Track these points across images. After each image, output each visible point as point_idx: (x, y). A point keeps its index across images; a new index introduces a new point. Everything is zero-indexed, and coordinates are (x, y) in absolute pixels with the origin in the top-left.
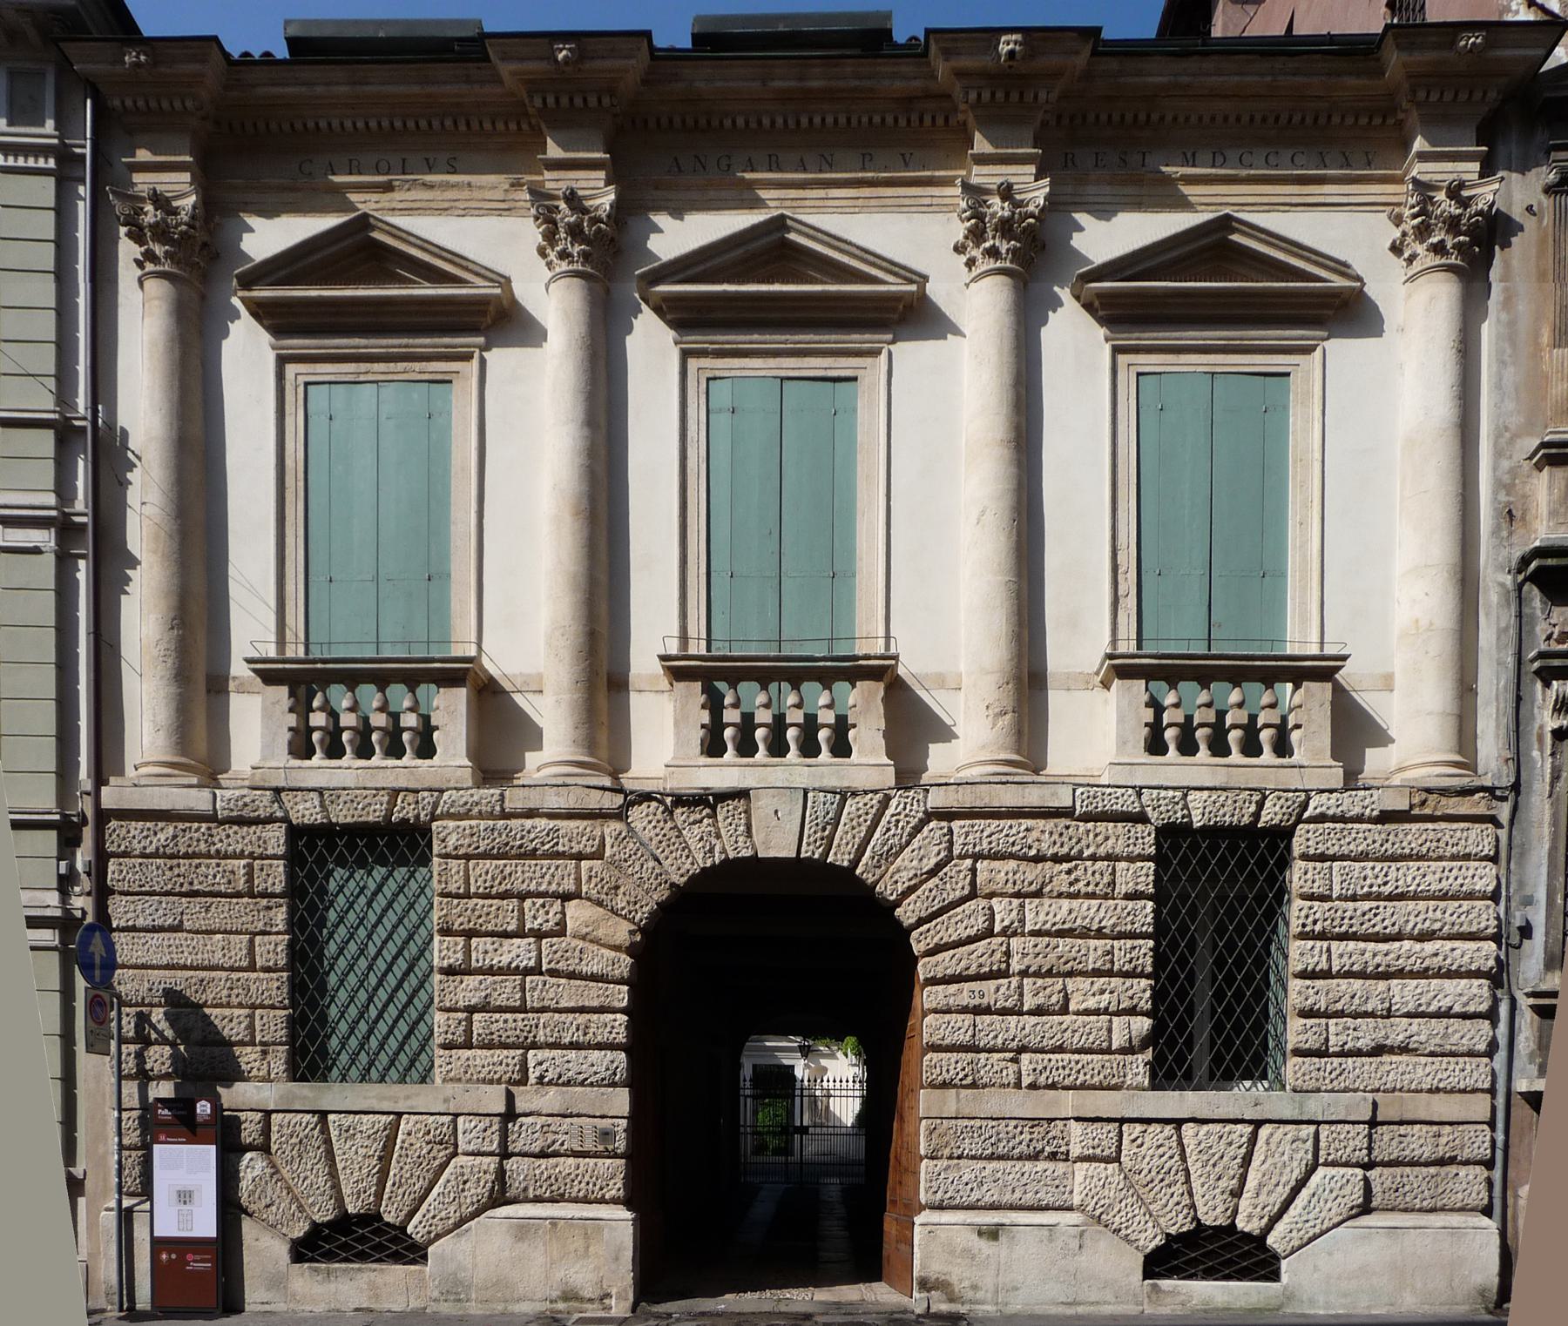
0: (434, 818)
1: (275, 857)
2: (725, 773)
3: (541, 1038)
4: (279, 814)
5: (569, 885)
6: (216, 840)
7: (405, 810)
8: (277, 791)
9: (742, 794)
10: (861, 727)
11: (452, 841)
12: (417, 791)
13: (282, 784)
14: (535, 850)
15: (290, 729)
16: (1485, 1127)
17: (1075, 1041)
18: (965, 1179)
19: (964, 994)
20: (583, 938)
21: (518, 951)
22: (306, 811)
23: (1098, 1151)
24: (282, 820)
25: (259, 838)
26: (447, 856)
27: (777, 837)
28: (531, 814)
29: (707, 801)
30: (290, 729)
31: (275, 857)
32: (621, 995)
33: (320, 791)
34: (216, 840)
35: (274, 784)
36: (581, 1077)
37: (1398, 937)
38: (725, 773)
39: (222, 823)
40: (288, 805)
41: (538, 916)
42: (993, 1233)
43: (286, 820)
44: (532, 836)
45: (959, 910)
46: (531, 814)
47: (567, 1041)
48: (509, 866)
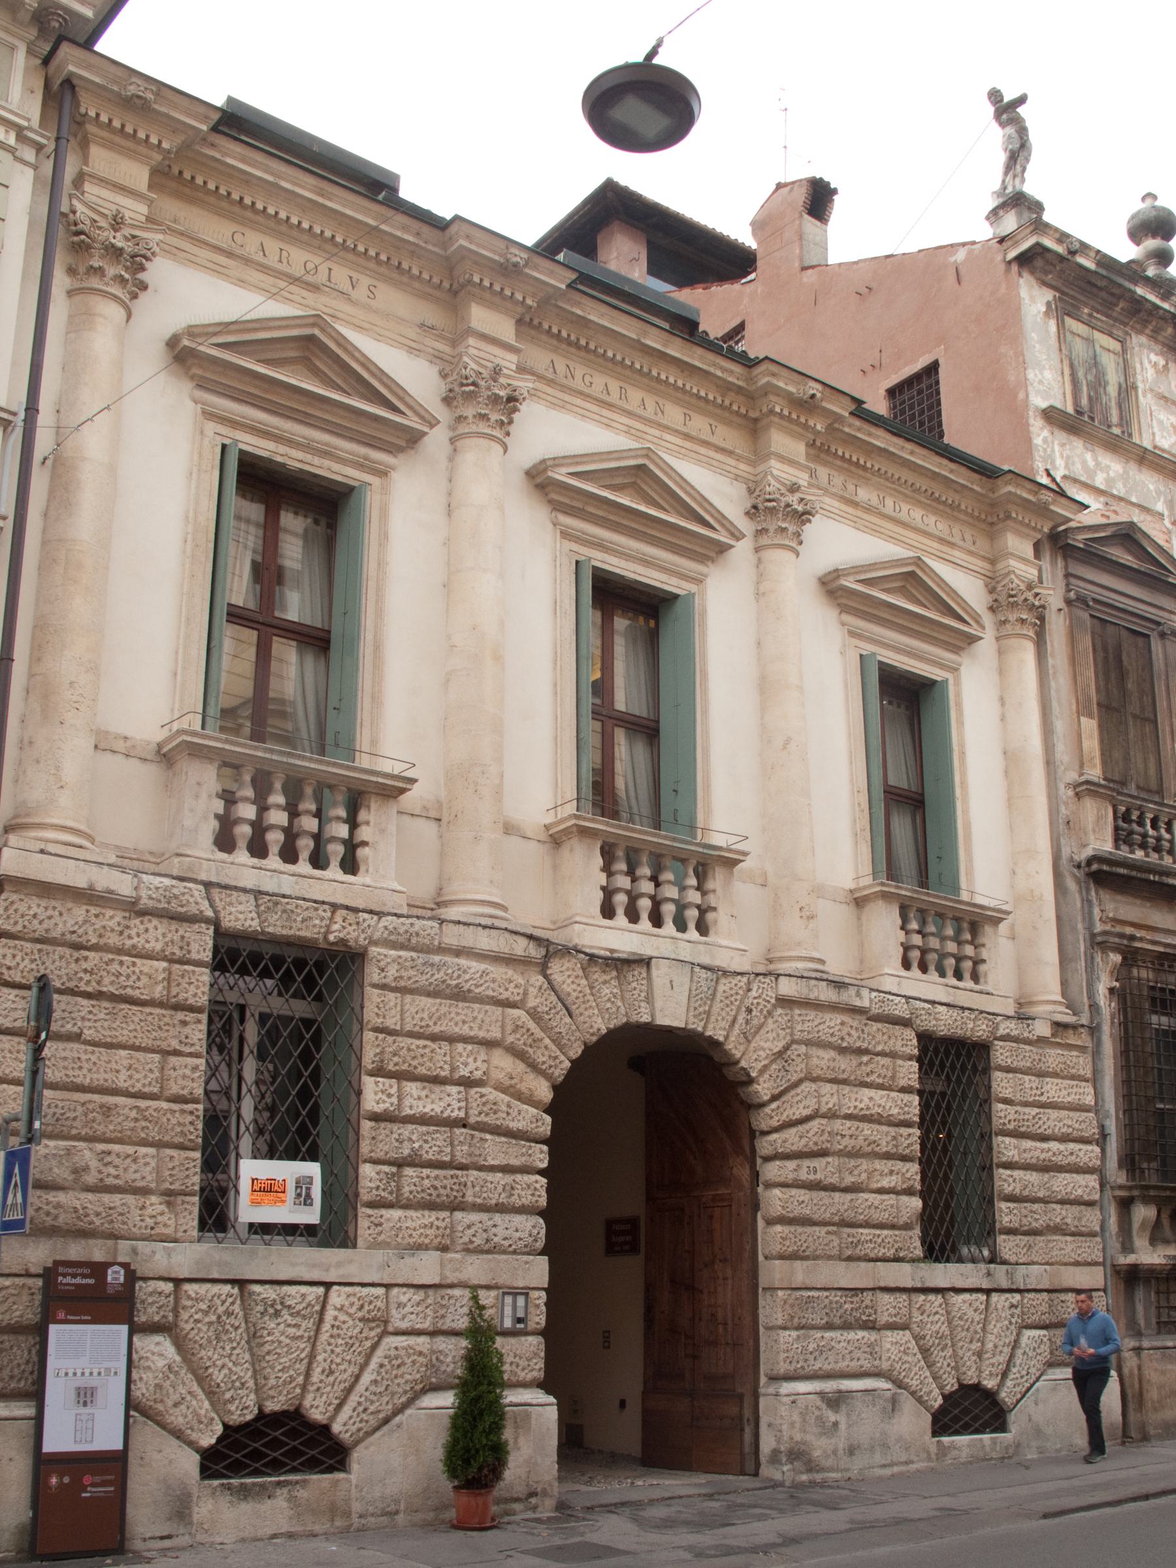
0: (374, 943)
1: (199, 964)
2: (620, 937)
3: (469, 1198)
4: (210, 913)
5: (496, 1033)
6: (133, 932)
7: (341, 930)
8: (208, 885)
9: (645, 962)
10: (720, 909)
11: (392, 972)
12: (355, 910)
13: (214, 879)
14: (469, 991)
15: (217, 816)
16: (1102, 1293)
17: (878, 1217)
18: (811, 1348)
19: (804, 1170)
20: (504, 1090)
21: (446, 1102)
22: (241, 916)
23: (897, 1319)
24: (207, 921)
25: (183, 937)
26: (384, 987)
27: (670, 1006)
28: (458, 952)
29: (623, 965)
30: (217, 816)
31: (199, 964)
32: (540, 1156)
33: (258, 893)
34: (133, 932)
35: (203, 876)
36: (506, 1243)
37: (1044, 1138)
38: (620, 937)
39: (143, 913)
40: (219, 905)
41: (471, 1062)
42: (835, 1401)
43: (216, 923)
44: (467, 977)
45: (799, 1090)
46: (458, 952)
47: (494, 1202)
48: (444, 1006)
